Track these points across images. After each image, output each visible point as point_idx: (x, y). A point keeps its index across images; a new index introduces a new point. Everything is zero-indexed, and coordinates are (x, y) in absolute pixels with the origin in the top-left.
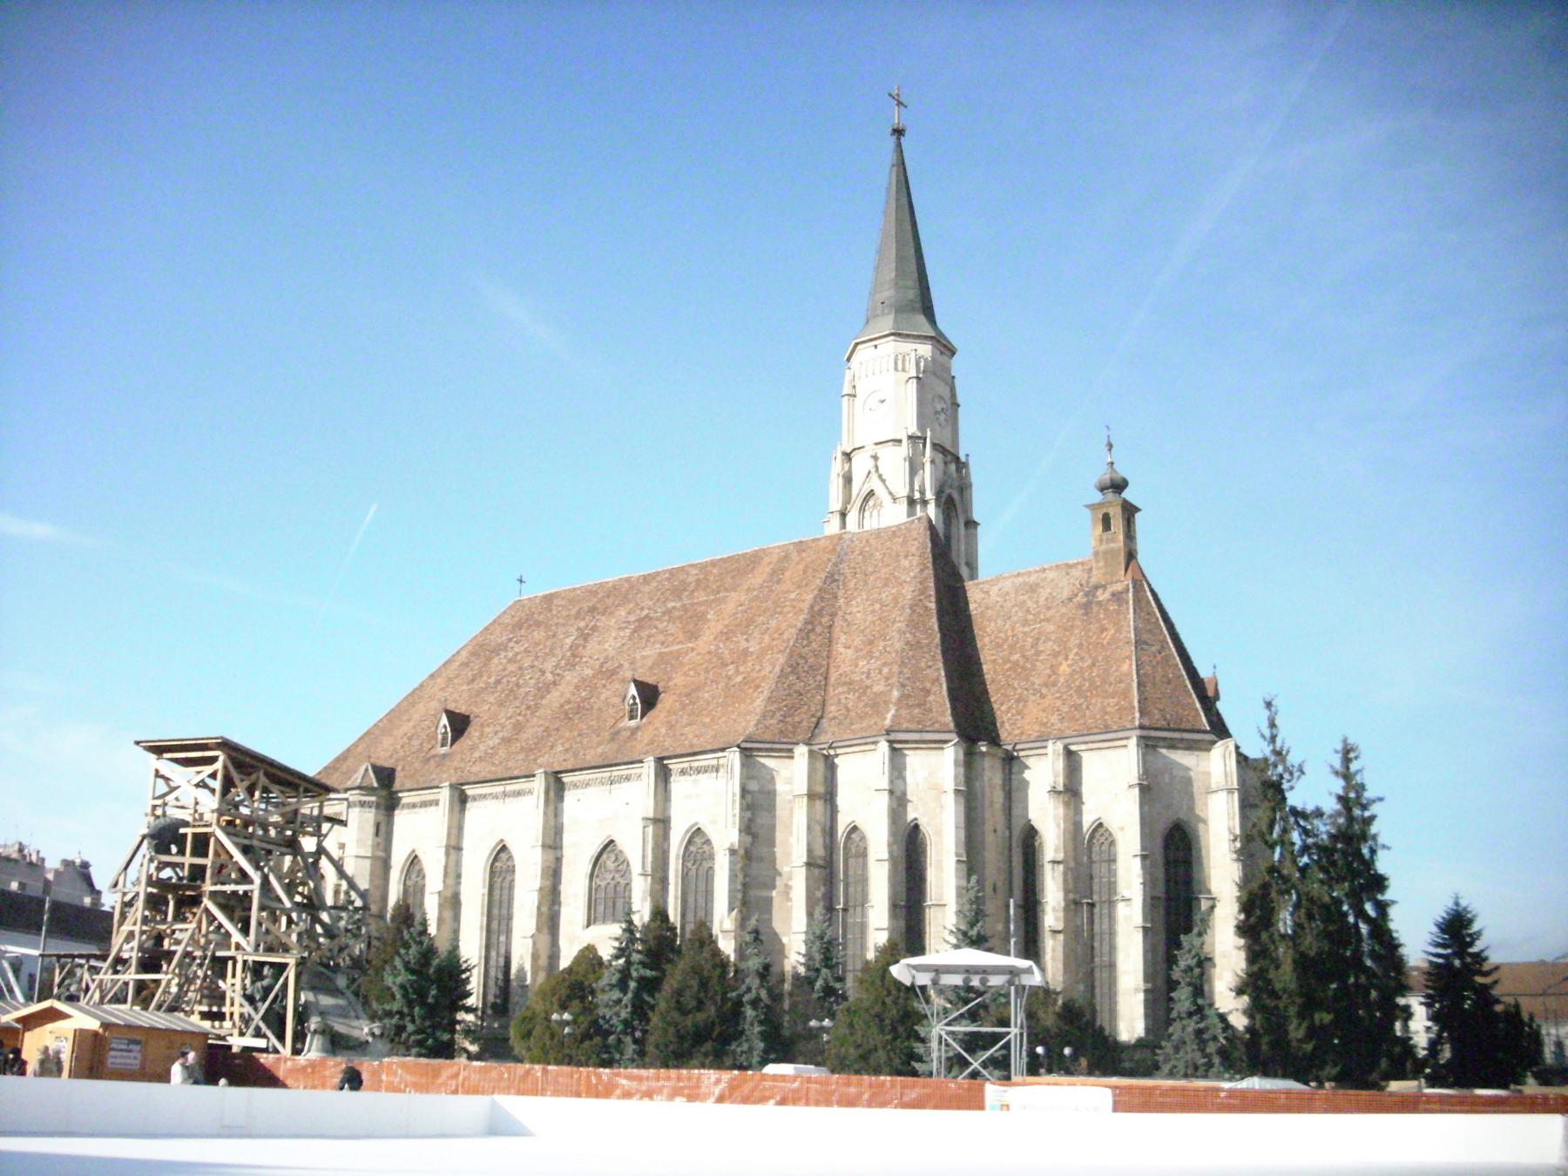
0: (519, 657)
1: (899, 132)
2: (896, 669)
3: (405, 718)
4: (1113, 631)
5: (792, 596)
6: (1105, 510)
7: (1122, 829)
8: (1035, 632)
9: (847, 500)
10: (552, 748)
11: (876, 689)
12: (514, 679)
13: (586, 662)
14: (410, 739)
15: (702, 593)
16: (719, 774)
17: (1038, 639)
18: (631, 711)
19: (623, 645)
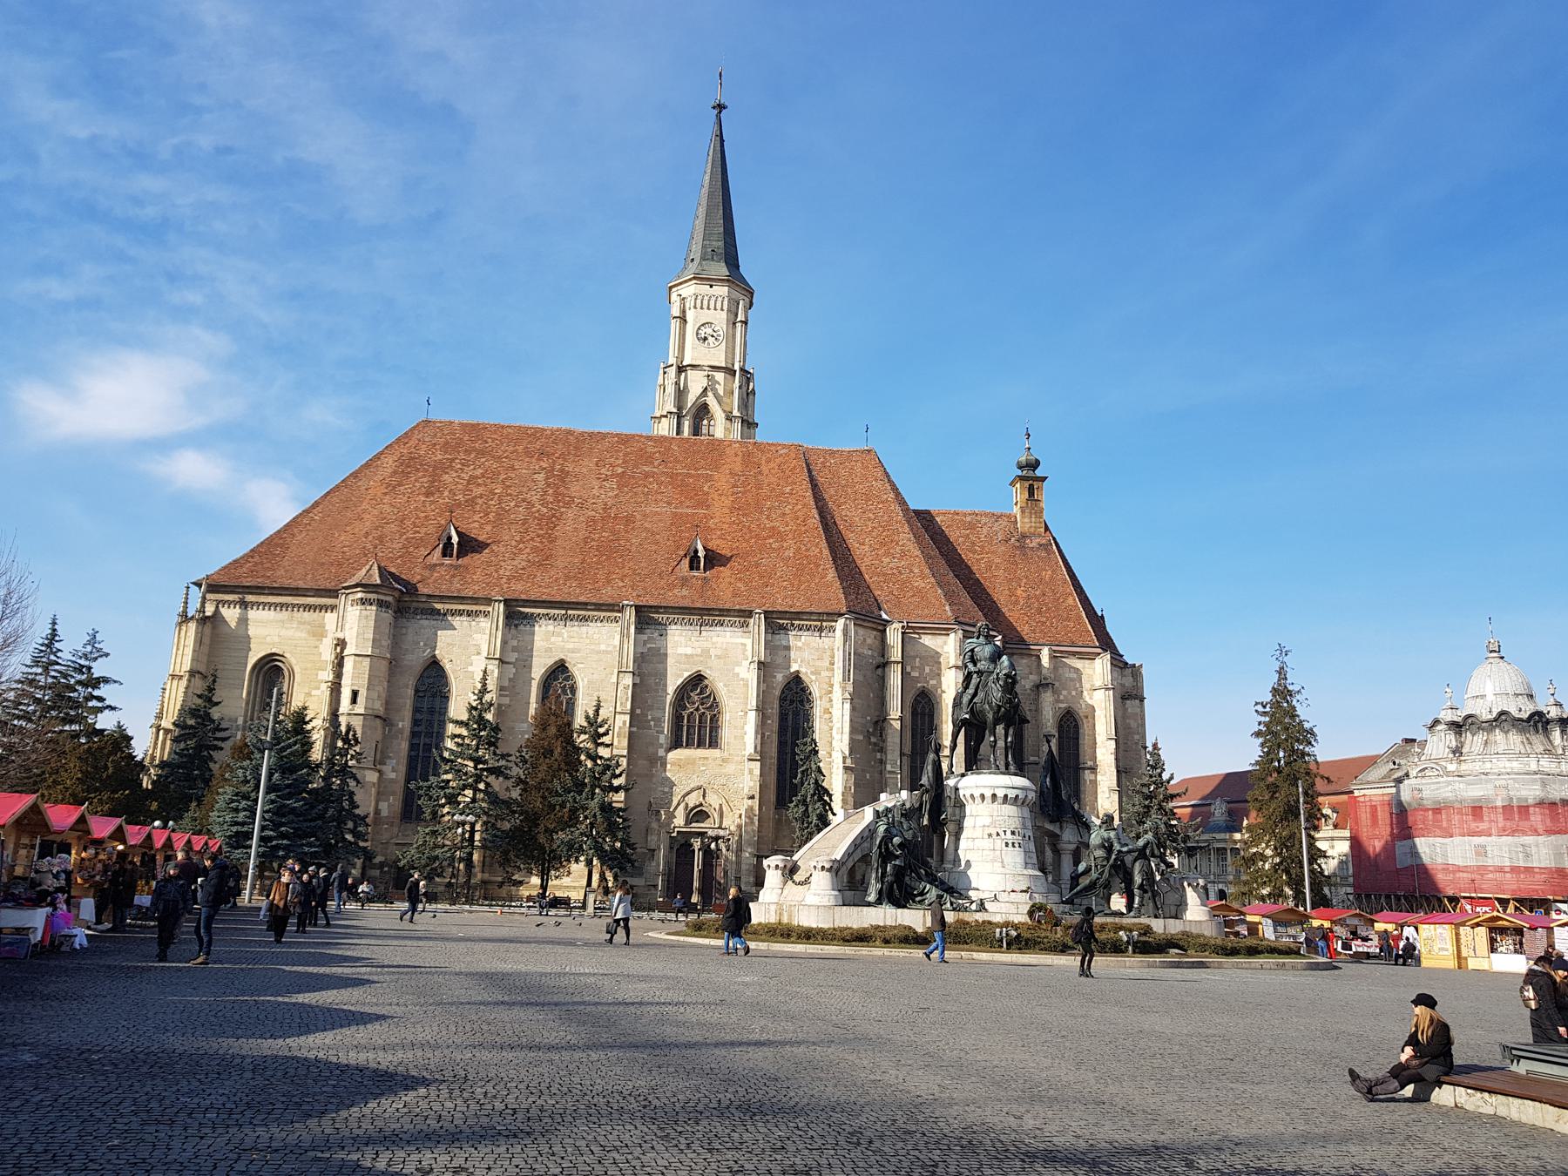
0: (480, 481)
1: (720, 107)
2: (927, 571)
4: (1050, 572)
6: (1031, 482)
7: (1087, 717)
9: (680, 408)
10: (609, 582)
12: (493, 502)
14: (381, 539)
16: (823, 634)
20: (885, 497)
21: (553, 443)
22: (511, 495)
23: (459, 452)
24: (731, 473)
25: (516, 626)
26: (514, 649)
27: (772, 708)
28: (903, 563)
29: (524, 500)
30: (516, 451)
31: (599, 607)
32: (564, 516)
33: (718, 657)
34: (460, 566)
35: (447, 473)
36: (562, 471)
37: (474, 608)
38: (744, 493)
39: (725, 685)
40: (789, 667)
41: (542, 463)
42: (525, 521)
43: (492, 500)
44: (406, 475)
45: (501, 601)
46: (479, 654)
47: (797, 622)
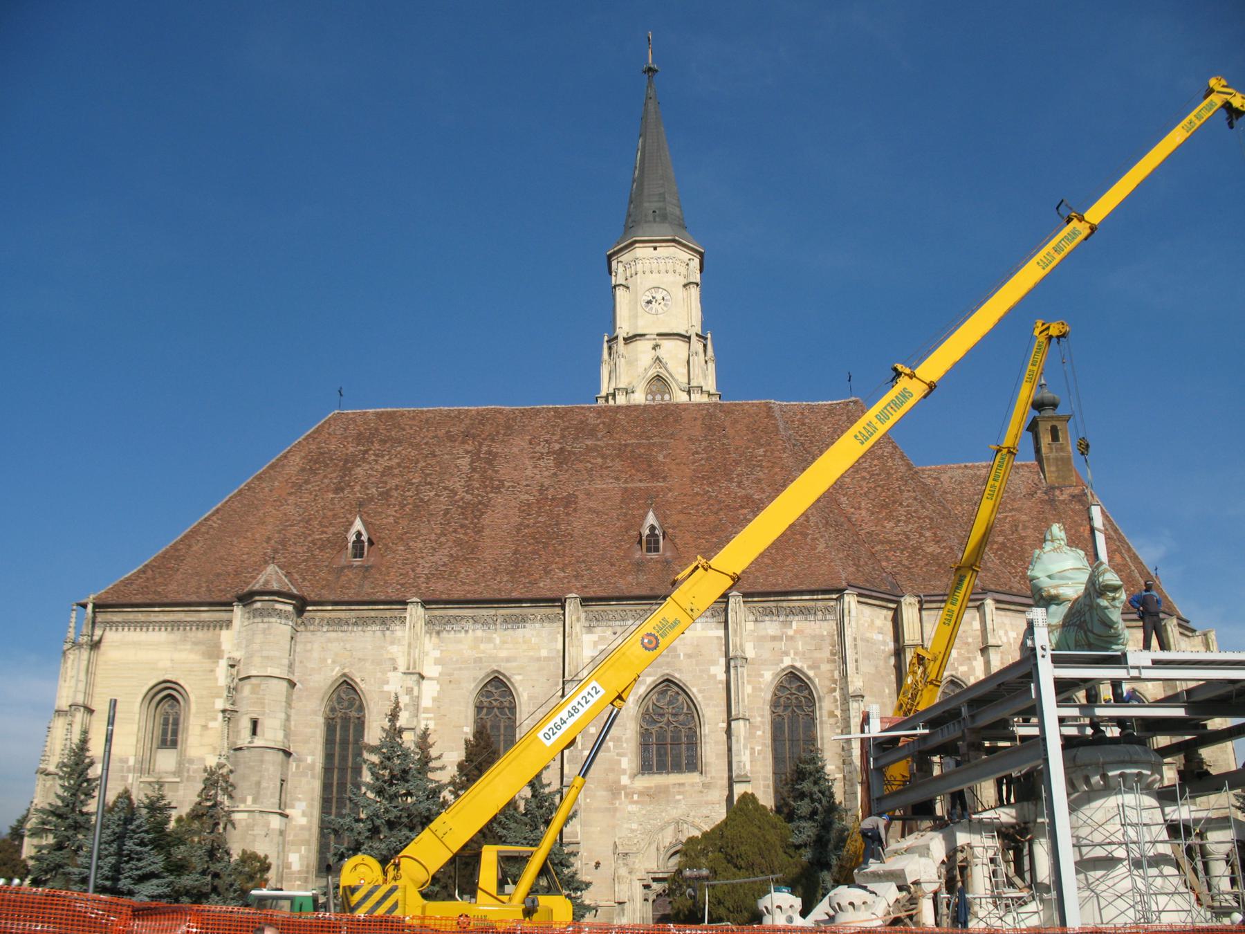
0: (396, 471)
3: (251, 519)
5: (761, 451)
8: (1009, 519)
10: (547, 572)
11: (929, 550)
12: (410, 493)
13: (512, 486)
15: (626, 436)
17: (1017, 526)
18: (648, 542)
19: (555, 474)
20: (880, 452)
21: (479, 423)
22: (430, 484)
23: (372, 443)
24: (690, 440)
25: (438, 633)
26: (438, 662)
27: (762, 716)
28: (910, 526)
29: (445, 488)
30: (436, 436)
31: (535, 601)
32: (492, 502)
33: (689, 656)
34: (371, 567)
35: (360, 466)
36: (490, 452)
37: (388, 614)
38: (708, 459)
39: (700, 691)
40: (782, 661)
41: (467, 447)
42: (447, 512)
43: (408, 491)
44: (314, 472)
45: (418, 602)
46: (395, 669)
47: (785, 604)
